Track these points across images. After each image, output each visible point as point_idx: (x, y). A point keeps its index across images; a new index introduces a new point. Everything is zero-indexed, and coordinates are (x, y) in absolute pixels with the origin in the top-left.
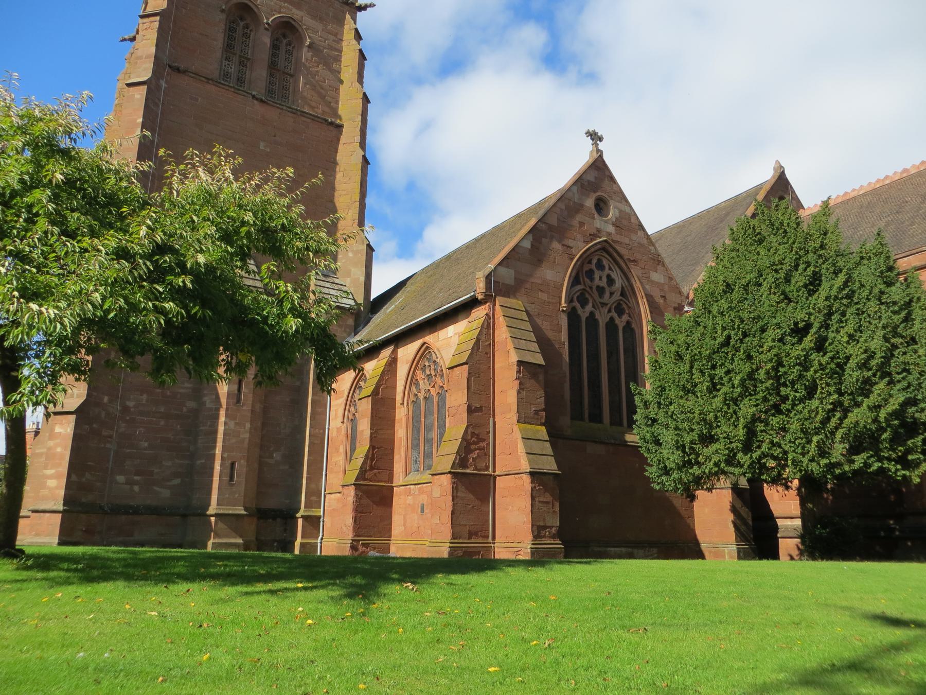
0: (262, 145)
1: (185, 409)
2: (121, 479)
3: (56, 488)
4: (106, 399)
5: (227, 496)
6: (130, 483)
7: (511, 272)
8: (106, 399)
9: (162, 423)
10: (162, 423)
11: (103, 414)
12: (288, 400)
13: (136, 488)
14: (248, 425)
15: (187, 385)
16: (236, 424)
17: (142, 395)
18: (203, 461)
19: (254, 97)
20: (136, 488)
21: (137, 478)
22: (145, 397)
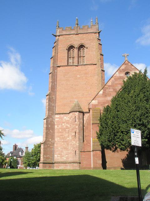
0: (78, 76)
4: (50, 140)
6: (58, 156)
7: (97, 101)
8: (50, 140)
9: (63, 143)
10: (63, 143)
11: (50, 143)
13: (59, 158)
14: (78, 142)
19: (75, 66)
20: (59, 158)
21: (59, 155)
22: (59, 138)
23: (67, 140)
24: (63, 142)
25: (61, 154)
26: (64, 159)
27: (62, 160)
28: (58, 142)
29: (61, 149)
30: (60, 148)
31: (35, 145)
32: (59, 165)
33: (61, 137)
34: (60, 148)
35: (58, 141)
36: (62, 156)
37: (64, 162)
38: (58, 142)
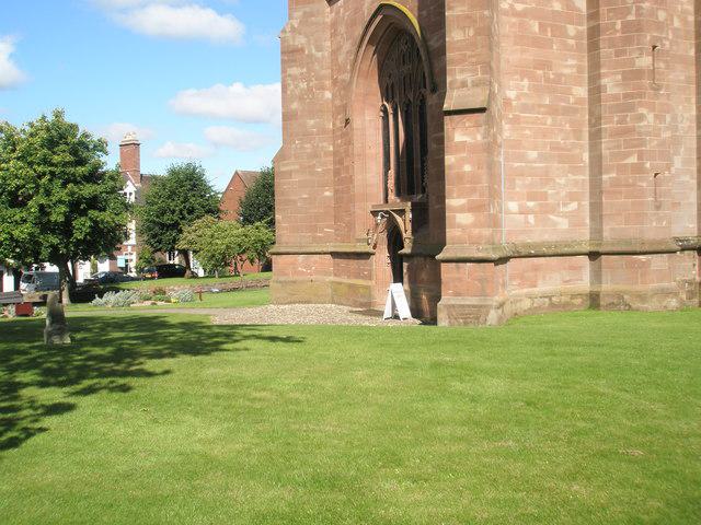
1: (572, 100)
2: (513, 206)
3: (474, 225)
5: (654, 224)
6: (524, 211)
10: (549, 121)
12: (683, 78)
13: (531, 218)
15: (571, 62)
16: (656, 117)
17: (522, 80)
18: (614, 175)
20: (531, 218)
21: (531, 204)
23: (572, 100)
24: (553, 111)
25: (544, 196)
26: (559, 227)
27: (546, 237)
28: (525, 108)
29: (542, 158)
30: (533, 154)
31: (58, 115)
32: (536, 269)
33: (540, 72)
34: (533, 154)
35: (523, 101)
36: (546, 210)
37: (566, 250)
38: (525, 108)
